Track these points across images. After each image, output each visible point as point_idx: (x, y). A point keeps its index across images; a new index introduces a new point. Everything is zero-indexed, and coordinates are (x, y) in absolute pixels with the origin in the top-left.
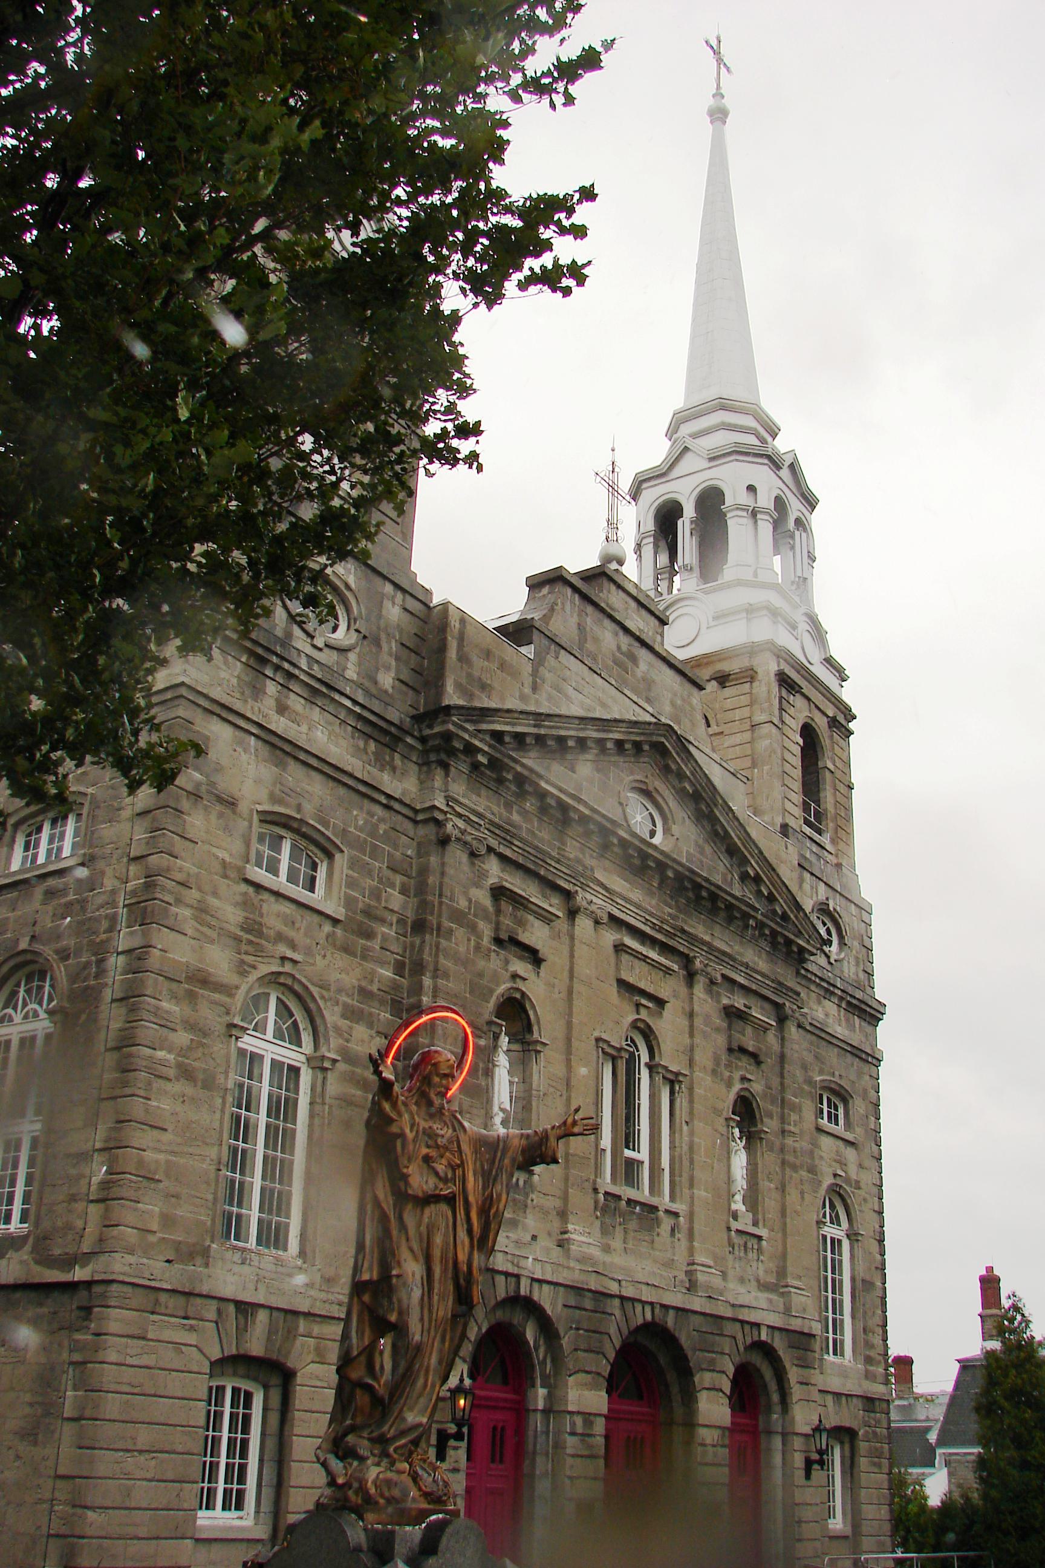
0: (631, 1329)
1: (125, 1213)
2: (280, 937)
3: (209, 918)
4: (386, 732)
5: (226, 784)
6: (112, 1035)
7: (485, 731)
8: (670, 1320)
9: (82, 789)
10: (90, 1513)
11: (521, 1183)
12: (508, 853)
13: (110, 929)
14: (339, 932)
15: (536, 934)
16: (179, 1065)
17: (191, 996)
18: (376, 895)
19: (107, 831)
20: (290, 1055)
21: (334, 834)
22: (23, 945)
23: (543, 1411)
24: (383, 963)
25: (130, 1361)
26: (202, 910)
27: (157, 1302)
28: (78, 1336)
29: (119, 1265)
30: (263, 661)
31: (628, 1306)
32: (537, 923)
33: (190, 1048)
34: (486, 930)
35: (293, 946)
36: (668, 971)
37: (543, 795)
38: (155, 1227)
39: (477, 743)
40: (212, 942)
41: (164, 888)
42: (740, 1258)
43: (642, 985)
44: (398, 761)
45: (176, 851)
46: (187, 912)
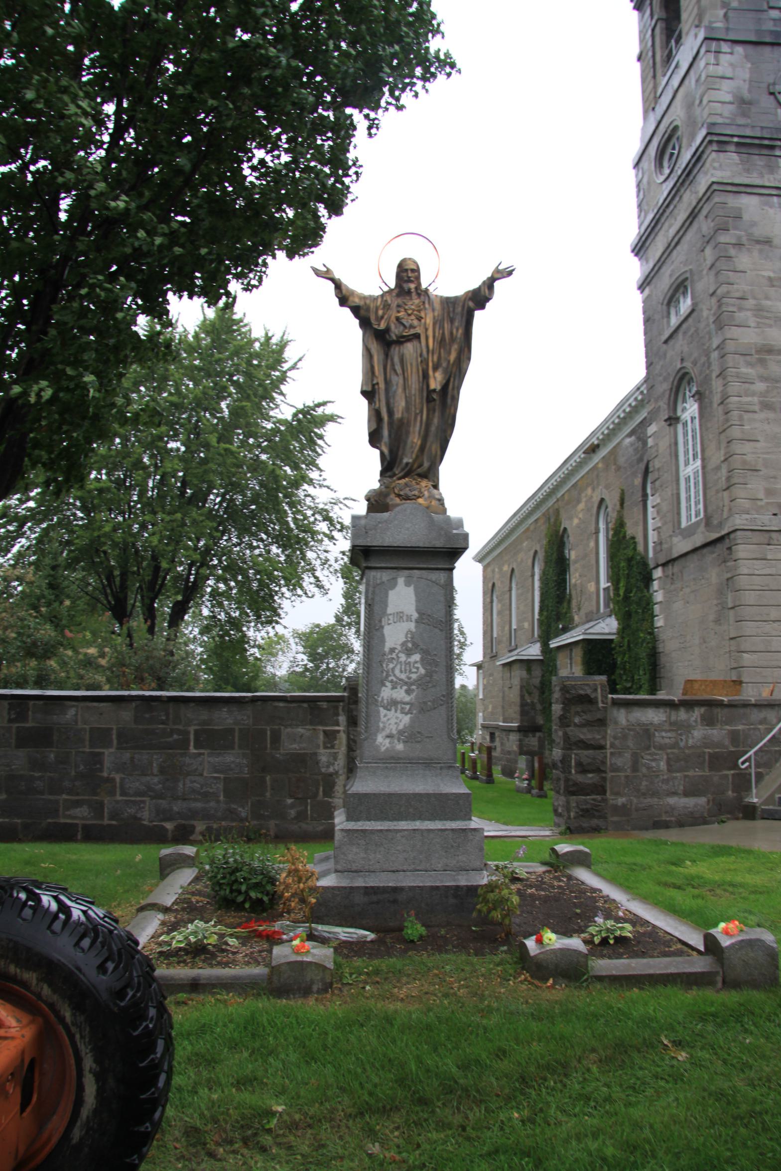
1: (738, 491)
3: (765, 314)
5: (757, 232)
6: (719, 395)
9: (686, 269)
10: (745, 655)
13: (710, 338)
16: (761, 403)
17: (762, 362)
19: (700, 286)
22: (679, 366)
25: (757, 572)
26: (759, 311)
27: (771, 538)
28: (729, 564)
29: (739, 521)
33: (767, 392)
38: (761, 495)
40: (770, 326)
41: (727, 304)
45: (731, 281)
46: (749, 313)
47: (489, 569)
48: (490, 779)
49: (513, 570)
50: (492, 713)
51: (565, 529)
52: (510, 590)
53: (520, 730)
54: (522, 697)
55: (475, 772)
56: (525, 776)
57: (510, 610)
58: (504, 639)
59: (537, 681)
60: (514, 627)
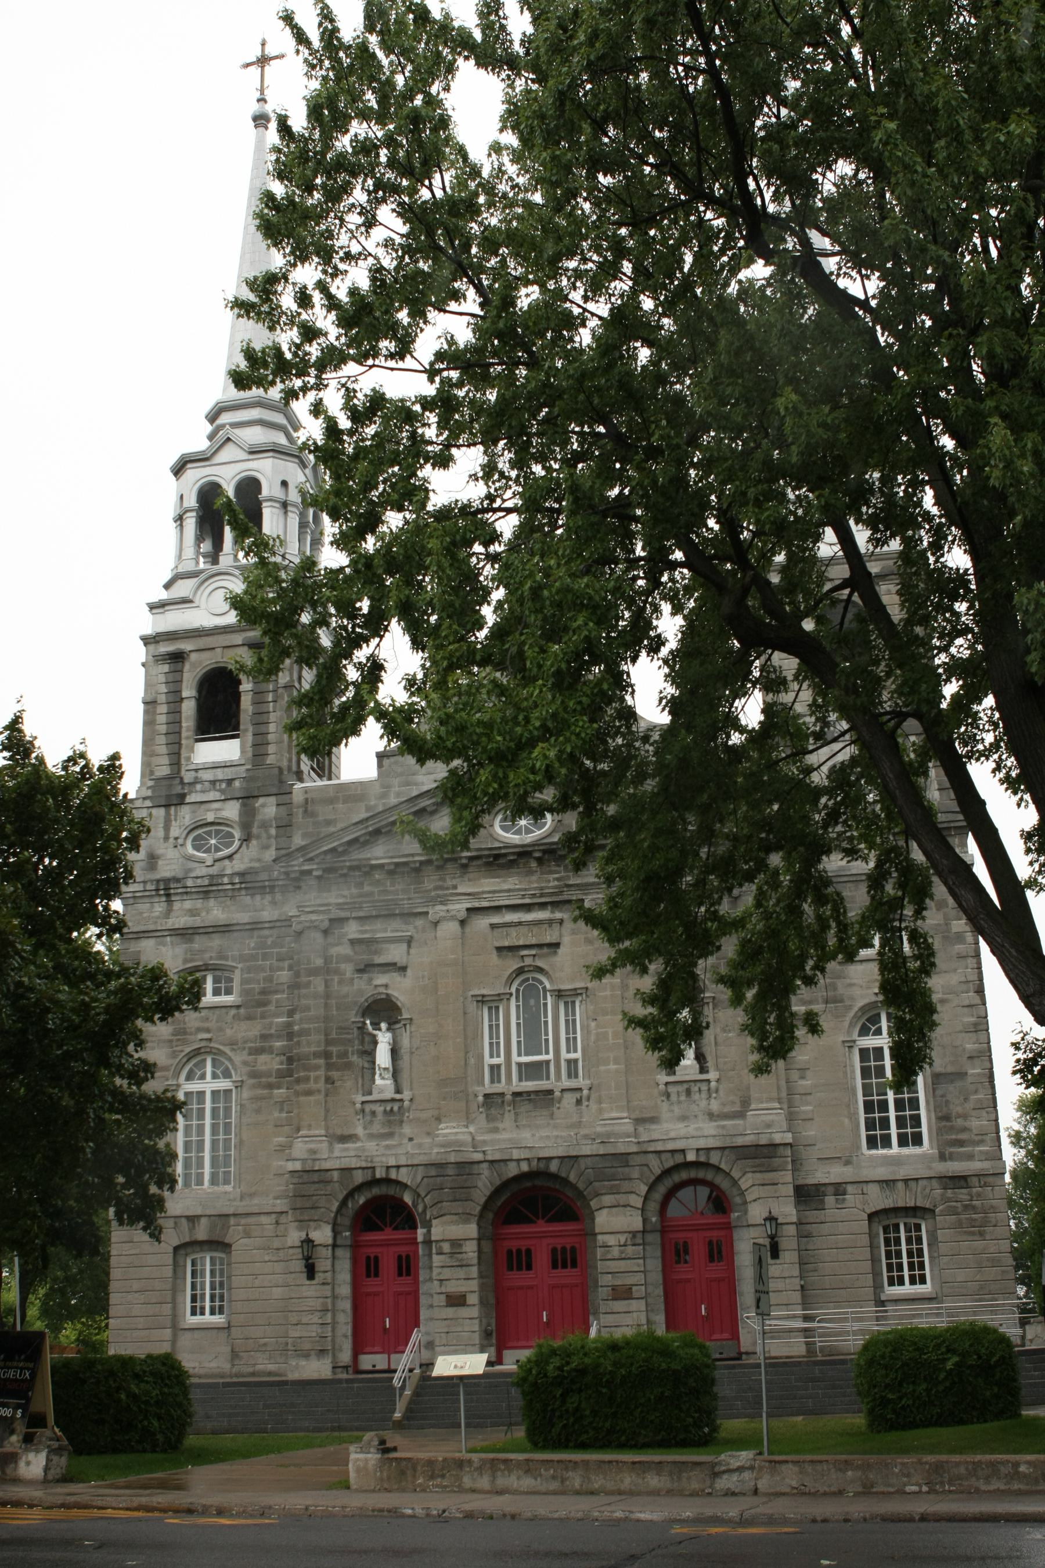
0: (505, 1178)
2: (199, 1030)
4: (264, 887)
7: (317, 856)
8: (554, 1167)
11: (396, 1108)
12: (361, 914)
14: (242, 1011)
15: (395, 953)
18: (269, 979)
20: (223, 1084)
21: (234, 960)
23: (423, 1242)
24: (278, 1016)
30: (168, 895)
31: (496, 1165)
32: (392, 946)
34: (348, 969)
35: (208, 1031)
36: (550, 922)
37: (382, 866)
39: (306, 868)
42: (679, 1102)
43: (521, 943)
44: (278, 897)
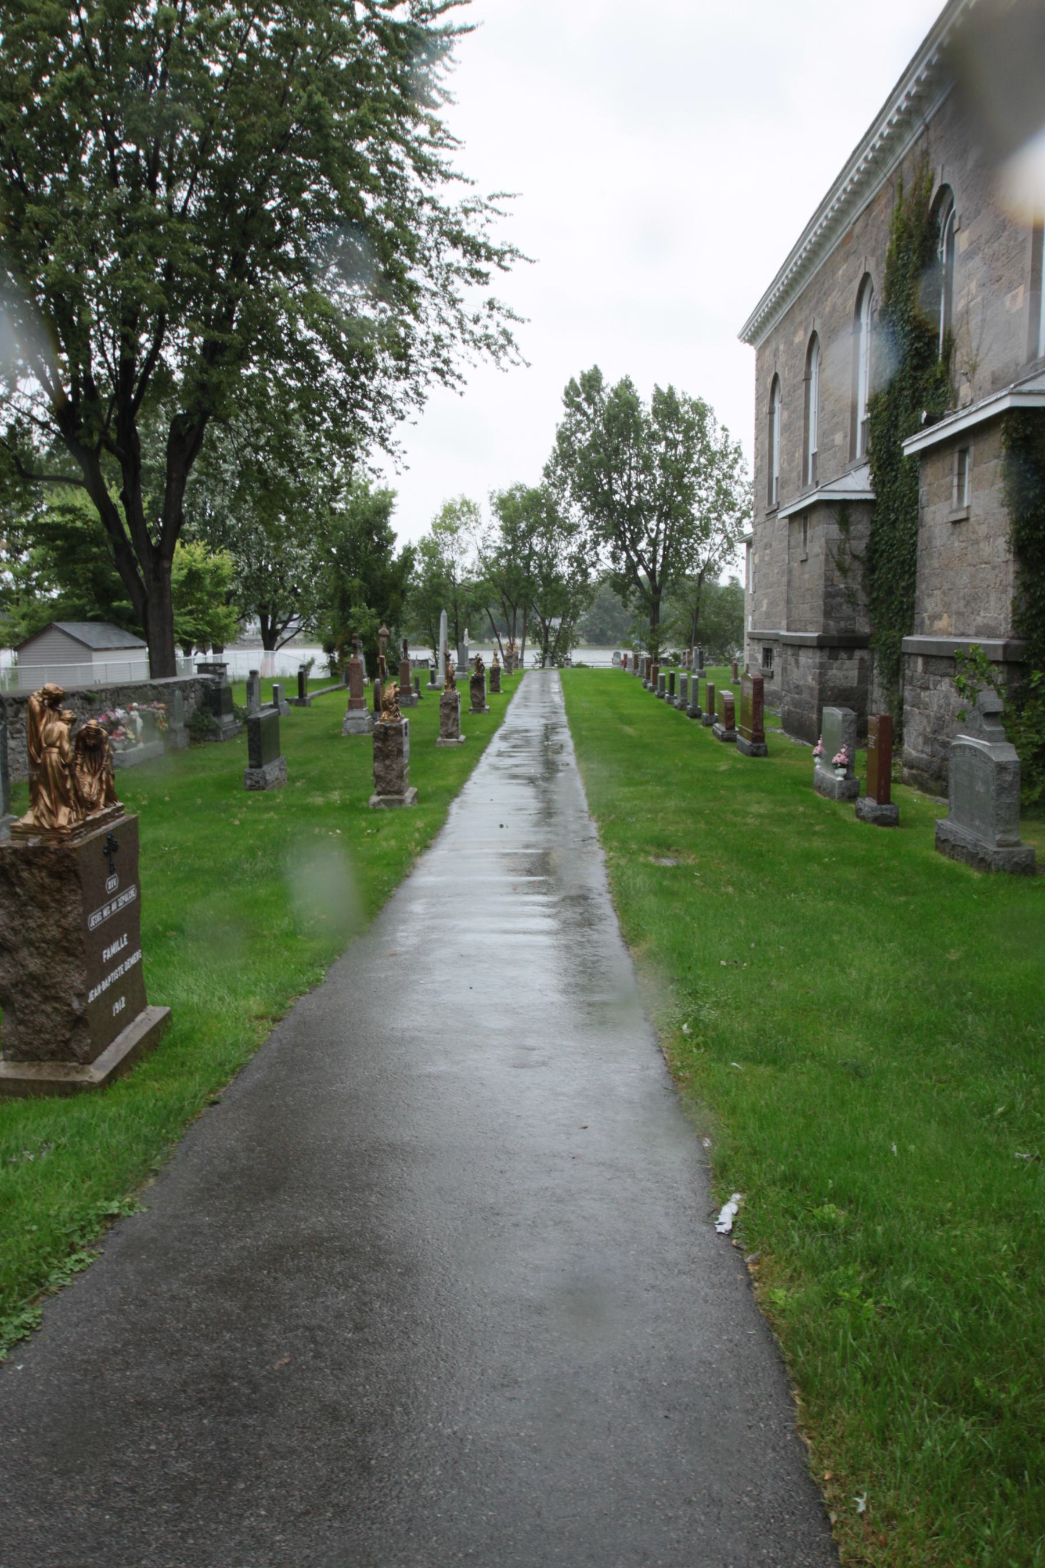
47: (768, 352)
48: (759, 746)
49: (814, 335)
50: (768, 615)
51: (945, 189)
52: (807, 379)
53: (822, 644)
54: (829, 580)
55: (731, 728)
56: (838, 758)
57: (807, 418)
58: (794, 475)
59: (860, 546)
60: (813, 449)
